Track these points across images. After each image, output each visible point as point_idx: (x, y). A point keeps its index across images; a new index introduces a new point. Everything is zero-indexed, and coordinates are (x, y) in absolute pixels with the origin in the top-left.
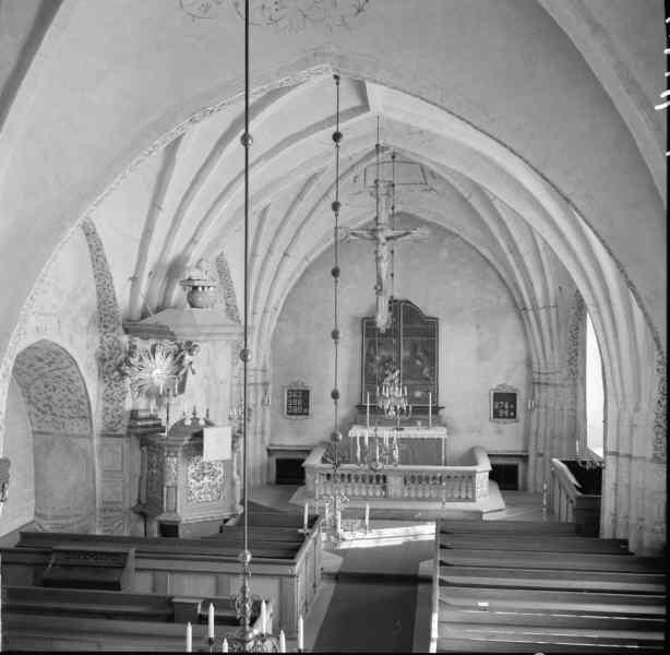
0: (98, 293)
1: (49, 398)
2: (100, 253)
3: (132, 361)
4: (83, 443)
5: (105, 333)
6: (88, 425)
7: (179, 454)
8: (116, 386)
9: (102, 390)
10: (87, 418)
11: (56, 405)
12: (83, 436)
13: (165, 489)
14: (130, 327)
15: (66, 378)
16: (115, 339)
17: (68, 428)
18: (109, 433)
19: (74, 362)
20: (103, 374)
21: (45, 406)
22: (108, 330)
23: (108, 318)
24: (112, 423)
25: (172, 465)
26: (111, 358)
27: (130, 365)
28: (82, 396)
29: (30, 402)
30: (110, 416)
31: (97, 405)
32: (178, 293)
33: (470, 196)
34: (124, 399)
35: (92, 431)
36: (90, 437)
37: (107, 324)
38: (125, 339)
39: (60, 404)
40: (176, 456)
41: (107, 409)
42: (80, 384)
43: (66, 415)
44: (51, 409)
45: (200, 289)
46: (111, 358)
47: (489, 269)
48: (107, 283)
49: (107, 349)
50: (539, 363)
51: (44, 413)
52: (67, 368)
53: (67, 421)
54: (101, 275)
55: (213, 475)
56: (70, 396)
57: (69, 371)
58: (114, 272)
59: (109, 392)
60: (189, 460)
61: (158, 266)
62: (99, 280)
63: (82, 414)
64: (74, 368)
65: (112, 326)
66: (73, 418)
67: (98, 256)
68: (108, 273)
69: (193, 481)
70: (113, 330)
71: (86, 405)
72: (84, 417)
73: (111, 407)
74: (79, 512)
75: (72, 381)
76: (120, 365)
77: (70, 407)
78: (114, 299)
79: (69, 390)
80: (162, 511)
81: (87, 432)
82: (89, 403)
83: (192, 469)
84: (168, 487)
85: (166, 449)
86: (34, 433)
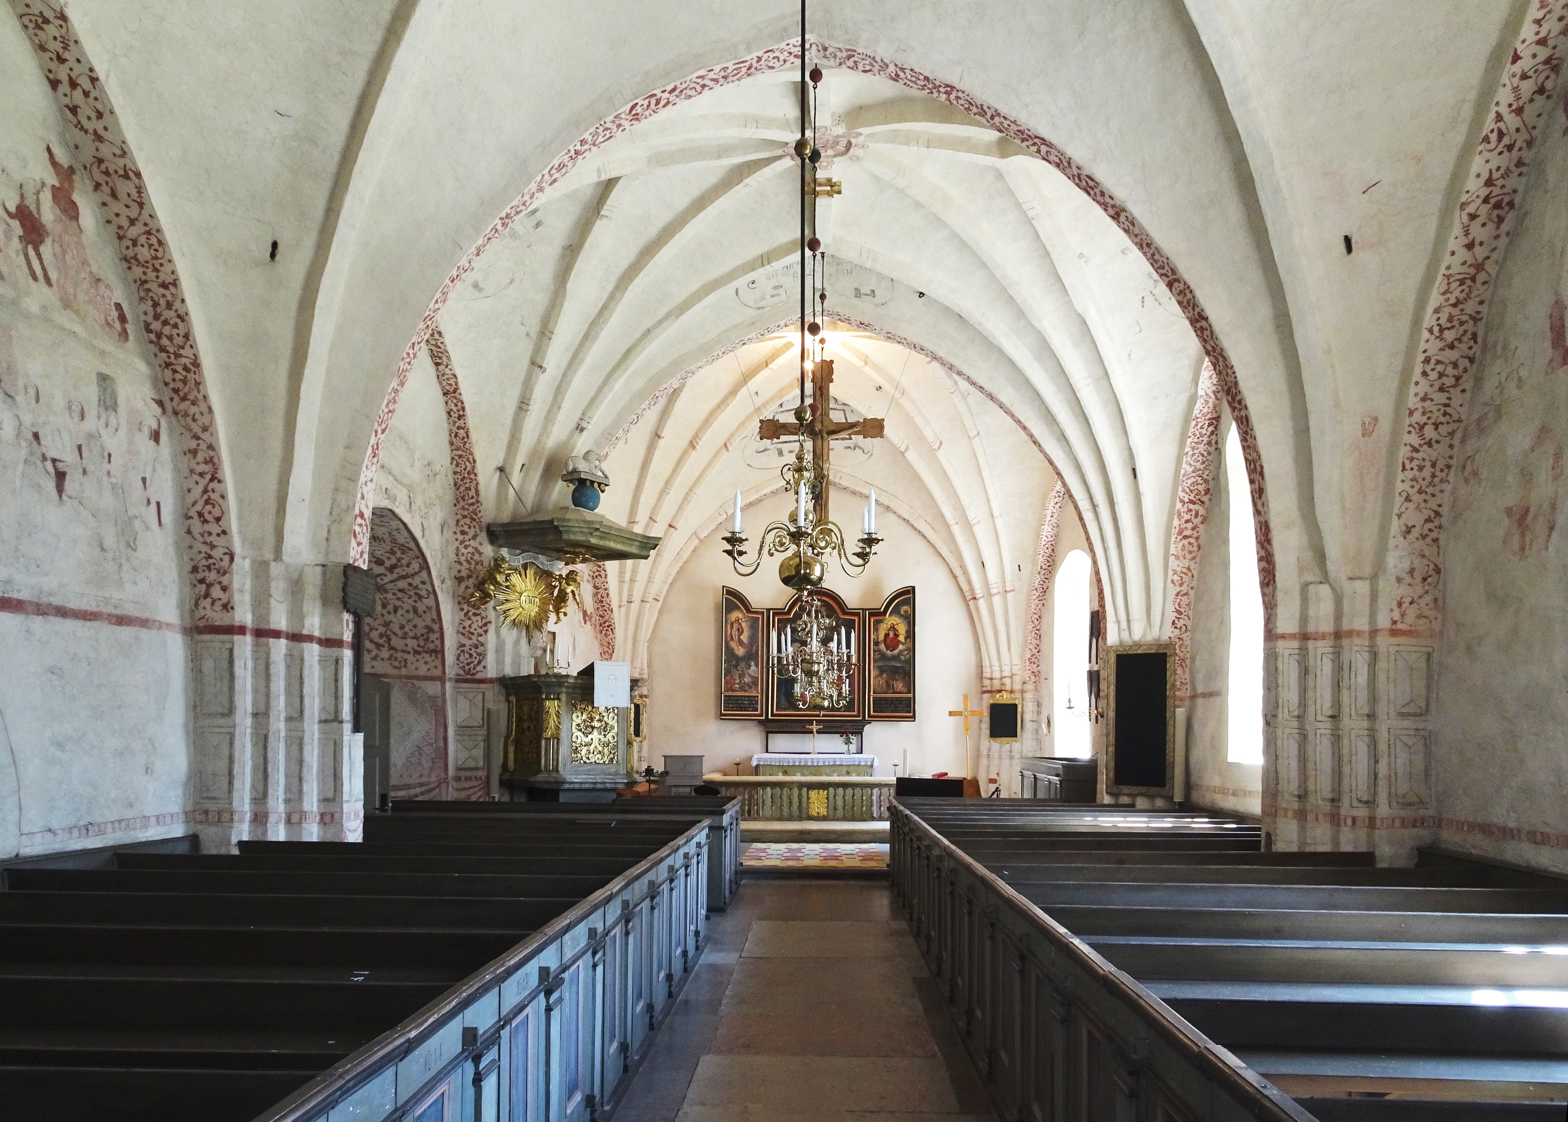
0: (455, 484)
1: (387, 624)
2: (460, 423)
3: (500, 578)
4: (432, 688)
6: (438, 662)
7: (563, 697)
8: (475, 615)
9: (457, 620)
10: (439, 652)
11: (396, 635)
12: (432, 679)
13: (543, 742)
14: (499, 534)
17: (411, 667)
19: (425, 566)
20: (462, 600)
21: (381, 636)
22: (467, 538)
24: (468, 664)
25: (552, 711)
26: (469, 577)
27: (497, 584)
28: (433, 620)
30: (467, 656)
31: (450, 642)
32: (561, 492)
33: (907, 448)
34: (486, 632)
36: (442, 679)
39: (400, 633)
40: (559, 699)
41: (463, 645)
42: (431, 602)
43: (409, 649)
44: (389, 640)
45: (588, 483)
46: (469, 577)
47: (1028, 171)
49: (466, 565)
50: (991, 666)
52: (413, 575)
53: (410, 658)
55: (605, 729)
56: (417, 621)
57: (416, 581)
58: (479, 453)
59: (467, 623)
60: (574, 706)
61: (535, 453)
63: (431, 646)
64: (424, 575)
65: (472, 532)
66: (419, 653)
67: (459, 428)
68: (471, 454)
69: (580, 734)
71: (437, 635)
72: (434, 651)
73: (468, 642)
74: (425, 779)
75: (420, 597)
76: (483, 583)
77: (415, 637)
79: (415, 611)
80: (539, 771)
81: (438, 672)
82: (441, 628)
83: (578, 718)
84: (548, 739)
85: (544, 689)
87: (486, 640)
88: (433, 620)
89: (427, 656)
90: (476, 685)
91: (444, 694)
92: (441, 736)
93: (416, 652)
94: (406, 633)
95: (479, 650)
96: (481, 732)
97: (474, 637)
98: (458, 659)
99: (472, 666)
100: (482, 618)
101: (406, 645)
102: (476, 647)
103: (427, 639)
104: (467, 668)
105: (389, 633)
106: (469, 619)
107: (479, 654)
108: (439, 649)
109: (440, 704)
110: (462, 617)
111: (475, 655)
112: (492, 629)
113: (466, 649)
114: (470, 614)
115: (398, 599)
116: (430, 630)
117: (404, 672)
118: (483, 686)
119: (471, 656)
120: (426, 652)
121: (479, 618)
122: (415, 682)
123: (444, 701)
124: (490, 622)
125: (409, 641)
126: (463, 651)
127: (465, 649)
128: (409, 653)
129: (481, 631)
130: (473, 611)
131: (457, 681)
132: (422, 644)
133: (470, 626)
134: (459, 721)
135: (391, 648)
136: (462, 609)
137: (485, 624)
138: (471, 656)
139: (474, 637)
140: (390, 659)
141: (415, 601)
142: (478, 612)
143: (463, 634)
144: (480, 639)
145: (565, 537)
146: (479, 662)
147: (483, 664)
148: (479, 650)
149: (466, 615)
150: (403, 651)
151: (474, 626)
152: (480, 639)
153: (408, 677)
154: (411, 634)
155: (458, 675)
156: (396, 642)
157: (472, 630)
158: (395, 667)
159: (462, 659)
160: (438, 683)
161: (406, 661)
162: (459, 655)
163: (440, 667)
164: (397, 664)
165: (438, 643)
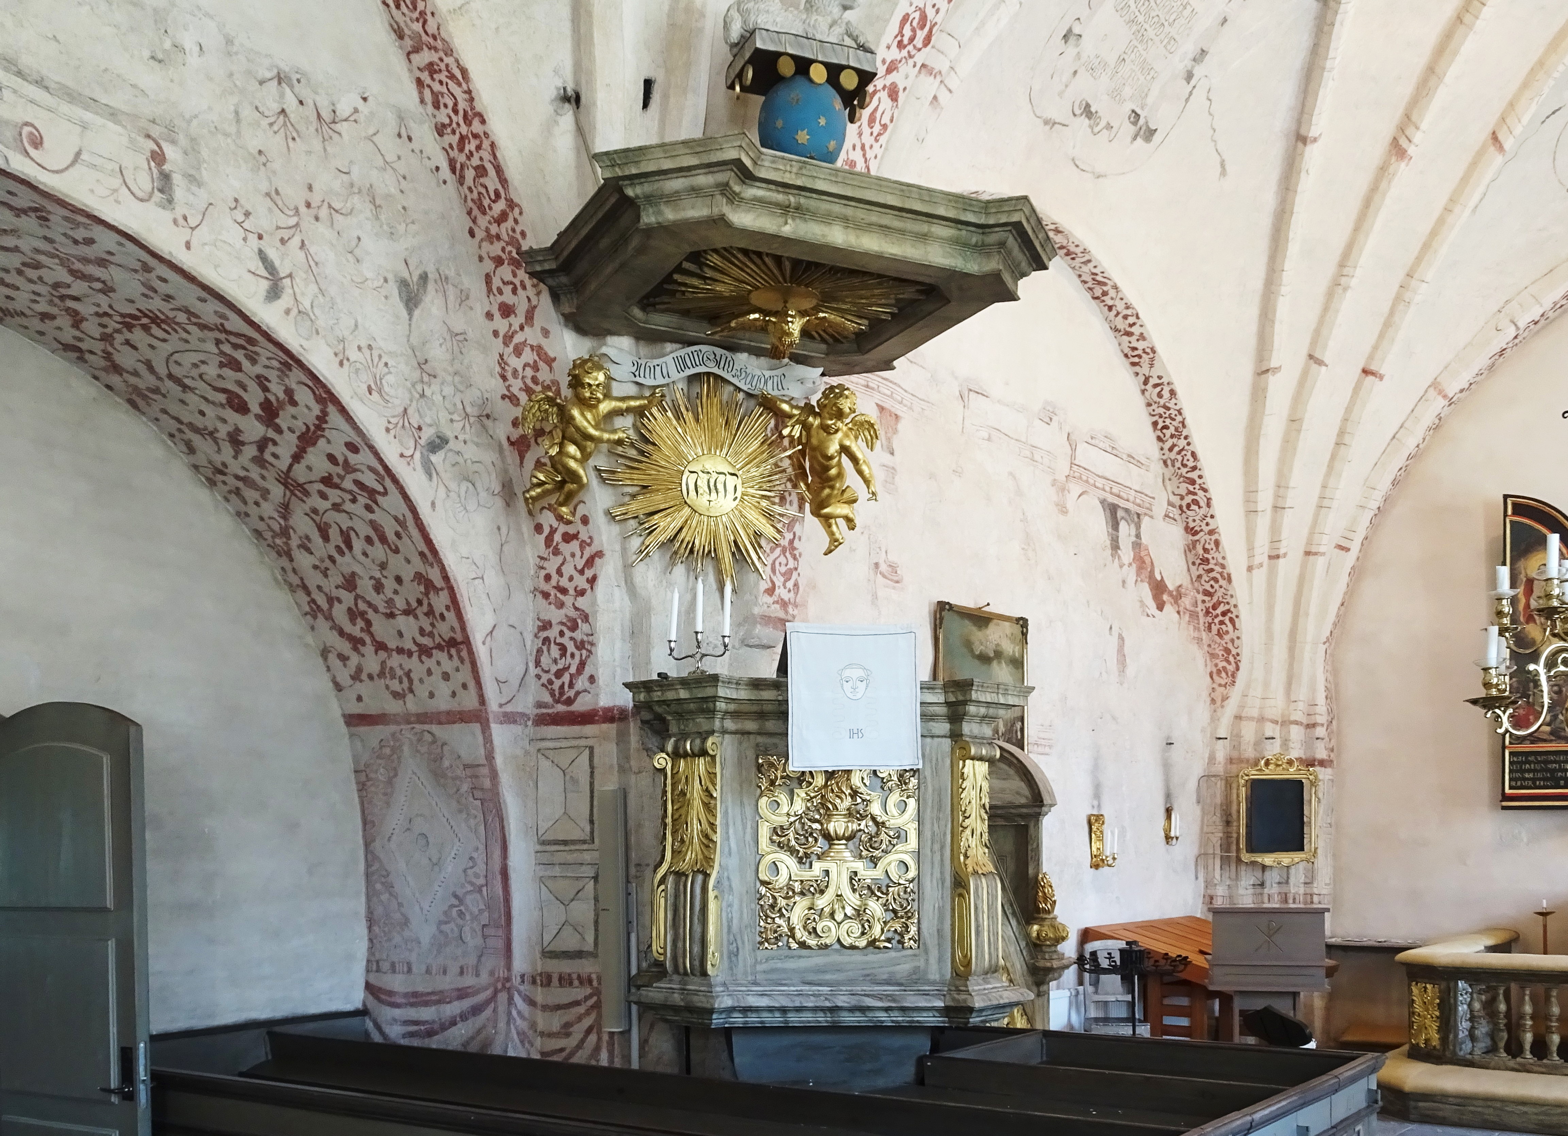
4: (463, 740)
5: (508, 339)
6: (465, 675)
8: (568, 538)
15: (348, 484)
16: (538, 350)
18: (562, 713)
21: (353, 614)
23: (505, 272)
24: (559, 674)
29: (314, 611)
30: (555, 652)
34: (592, 581)
35: (482, 701)
37: (508, 297)
38: (569, 346)
41: (546, 625)
48: (461, 97)
51: (356, 643)
54: (431, 68)
56: (396, 563)
62: (436, 105)
63: (444, 629)
70: (530, 317)
72: (452, 643)
73: (555, 615)
77: (407, 612)
78: (499, 170)
81: (469, 701)
82: (446, 578)
86: (354, 720)
87: (594, 603)
88: (422, 554)
89: (442, 656)
90: (576, 729)
91: (490, 756)
92: (497, 867)
93: (424, 651)
94: (390, 602)
95: (578, 635)
96: (587, 857)
97: (568, 600)
98: (538, 663)
99: (566, 678)
100: (583, 545)
101: (400, 634)
102: (574, 627)
103: (430, 613)
104: (557, 683)
105: (362, 606)
106: (556, 552)
107: (580, 646)
108: (459, 637)
109: (487, 783)
110: (542, 550)
111: (571, 647)
112: (608, 570)
113: (553, 633)
114: (557, 537)
115: (336, 507)
116: (429, 585)
117: (411, 705)
118: (589, 730)
119: (563, 649)
120: (439, 647)
121: (575, 545)
122: (434, 728)
123: (494, 775)
124: (600, 554)
125: (402, 622)
126: (546, 640)
127: (553, 633)
128: (410, 654)
129: (581, 582)
130: (562, 528)
131: (542, 720)
132: (428, 628)
133: (559, 572)
134: (544, 826)
135: (381, 646)
136: (539, 528)
137: (590, 563)
138: (563, 649)
139: (568, 600)
140: (382, 674)
141: (368, 508)
142: (571, 530)
143: (546, 595)
144: (581, 602)
145: (648, 218)
146: (582, 665)
147: (588, 670)
148: (578, 635)
149: (549, 540)
150: (400, 651)
151: (568, 570)
152: (581, 602)
153: (424, 718)
154: (400, 603)
155: (540, 705)
156: (382, 628)
157: (564, 582)
158: (396, 695)
159: (545, 660)
160: (476, 727)
161: (408, 674)
162: (539, 651)
163: (472, 684)
164: (395, 685)
165: (451, 616)
